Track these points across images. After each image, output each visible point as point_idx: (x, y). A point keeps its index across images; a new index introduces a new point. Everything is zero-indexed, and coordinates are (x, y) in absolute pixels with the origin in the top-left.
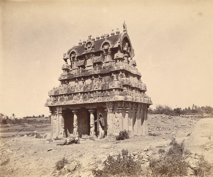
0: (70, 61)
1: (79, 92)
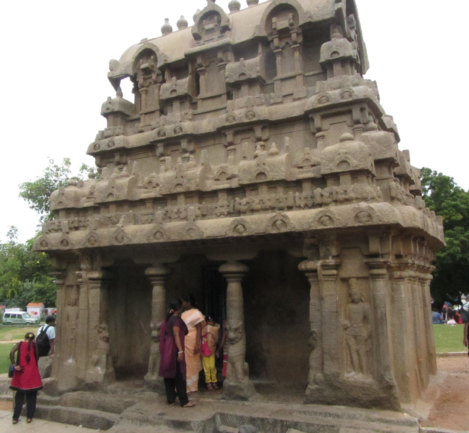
1: (179, 194)
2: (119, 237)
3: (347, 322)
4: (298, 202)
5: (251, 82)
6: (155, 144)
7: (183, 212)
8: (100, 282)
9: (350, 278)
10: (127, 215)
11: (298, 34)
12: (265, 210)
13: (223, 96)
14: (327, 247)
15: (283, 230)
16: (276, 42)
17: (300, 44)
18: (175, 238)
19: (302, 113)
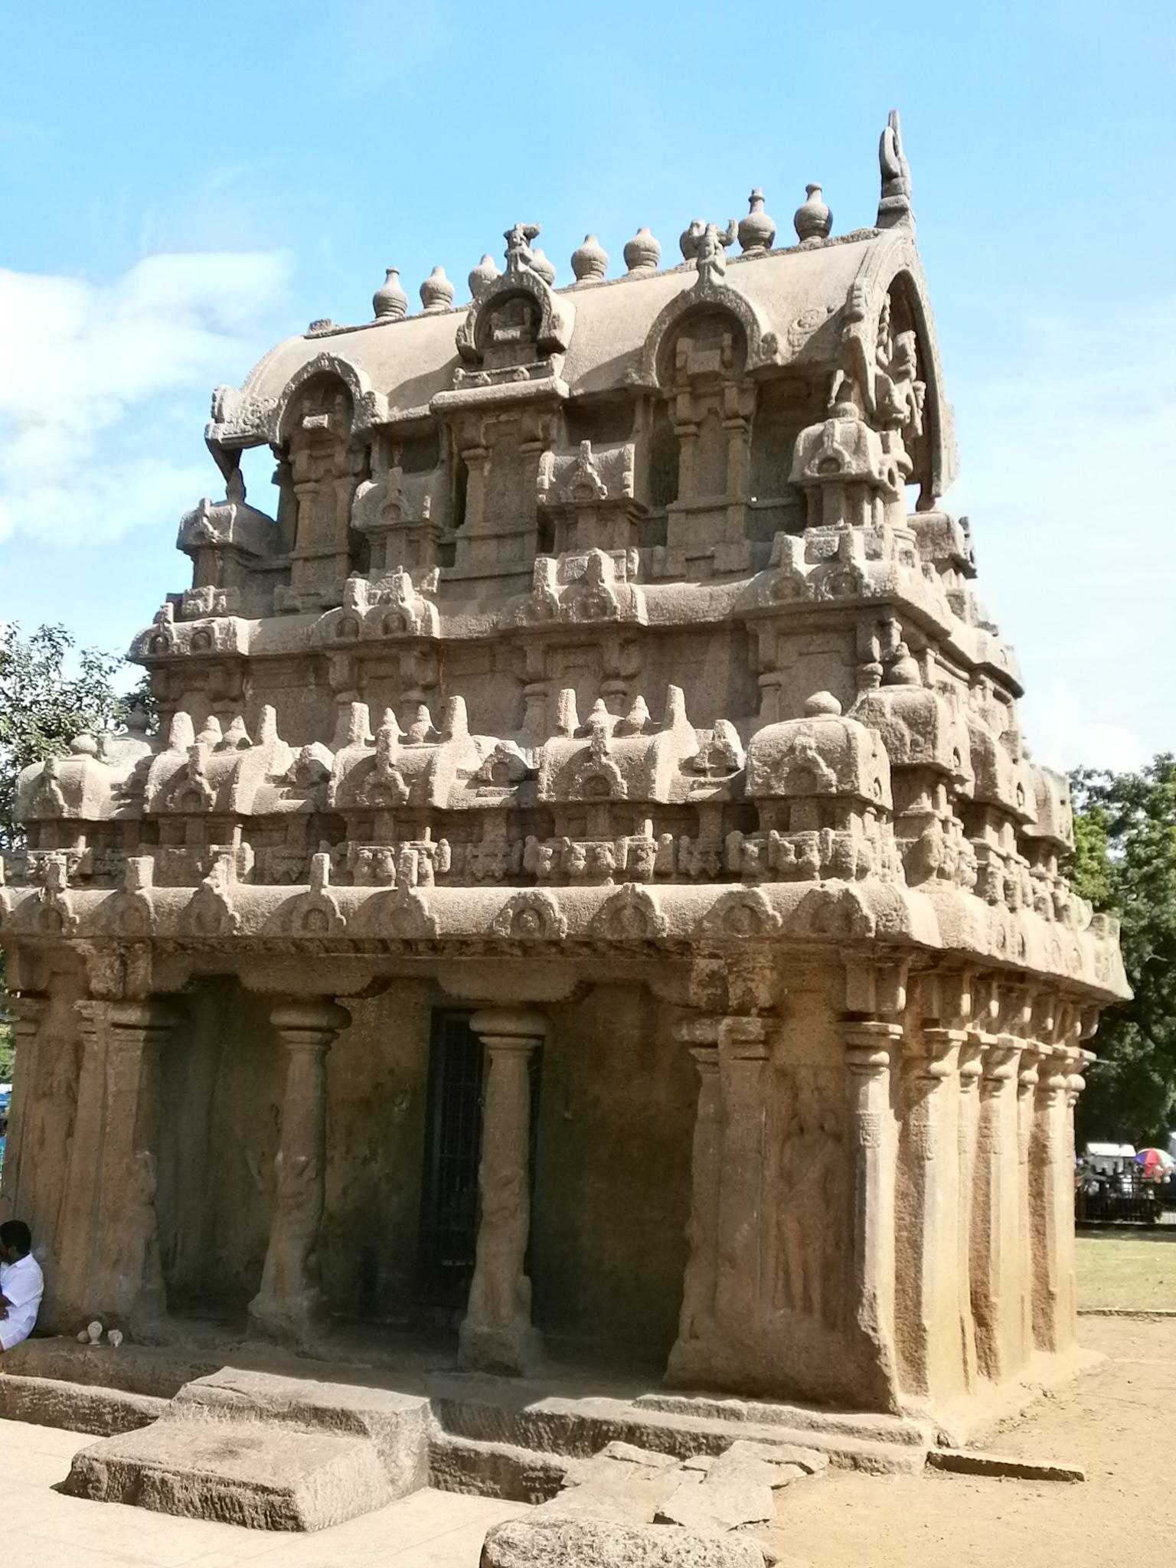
0: (272, 464)
6: (328, 654)
8: (141, 1034)
13: (526, 538)
14: (750, 984)
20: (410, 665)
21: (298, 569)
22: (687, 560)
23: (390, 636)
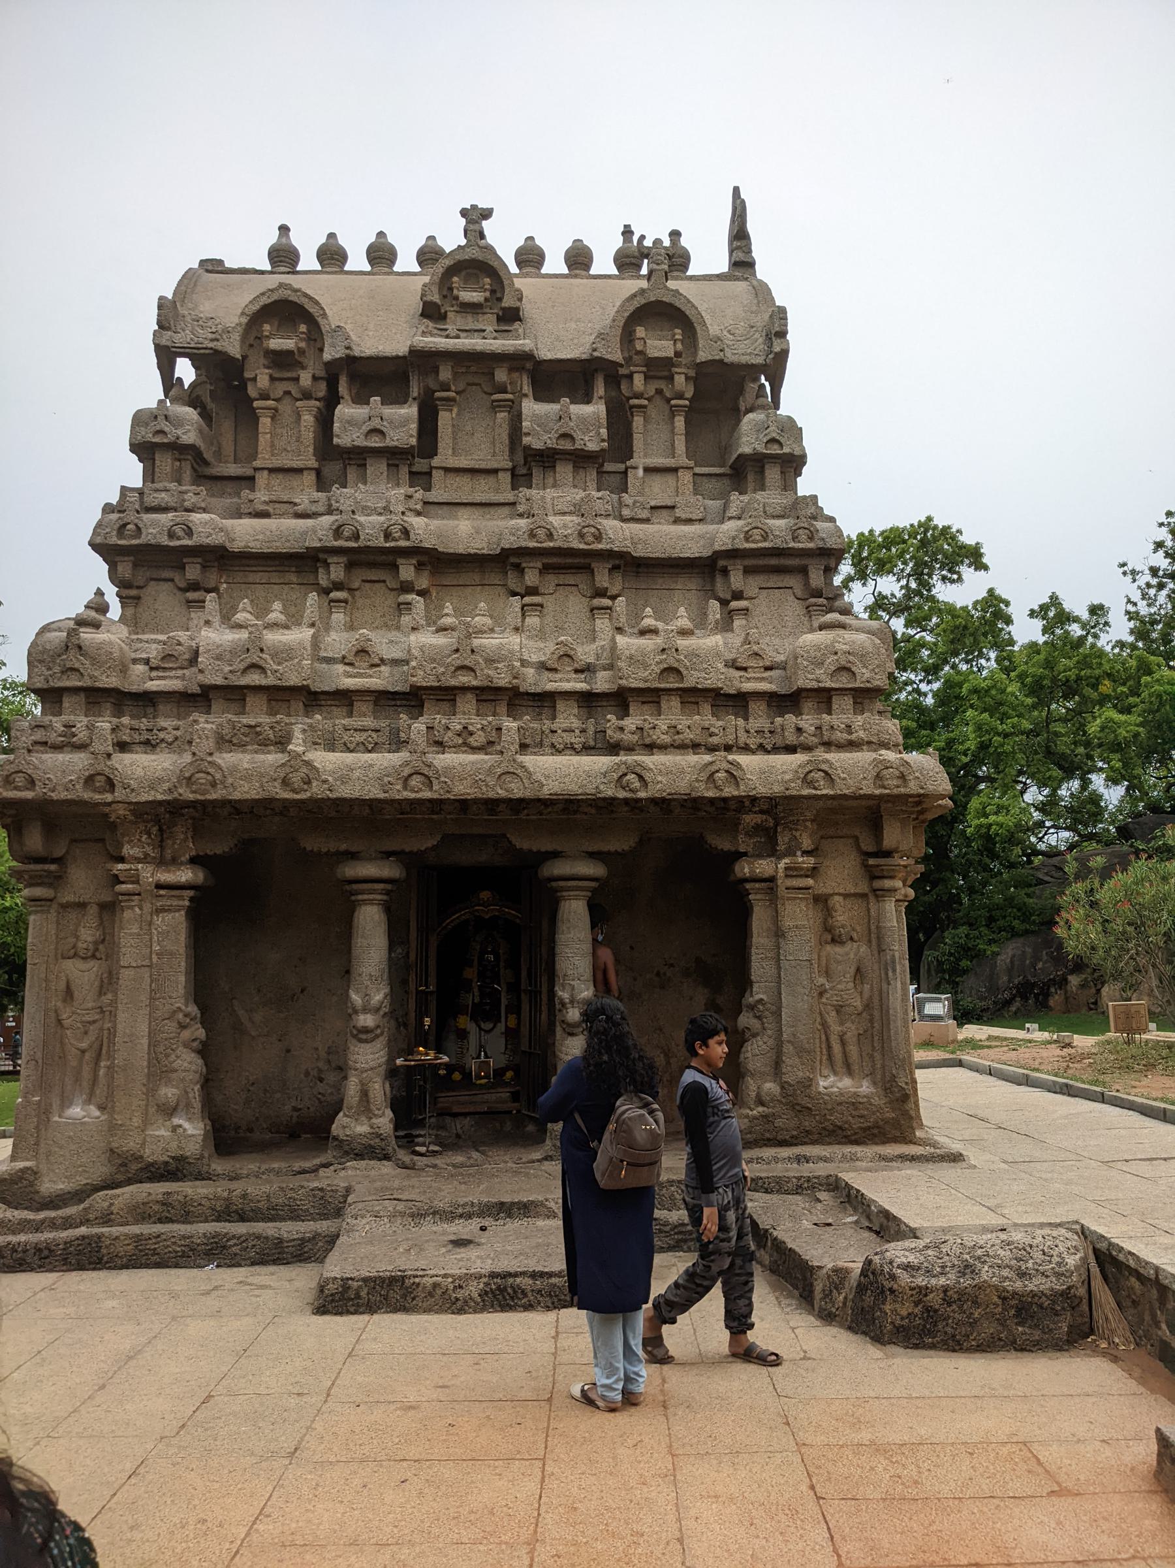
1: (464, 689)
2: (296, 779)
3: (822, 980)
4: (743, 738)
5: (581, 459)
7: (480, 733)
9: (832, 895)
10: (311, 726)
11: (687, 378)
12: (682, 747)
15: (729, 791)
16: (638, 381)
17: (690, 400)
18: (462, 789)
19: (707, 553)
20: (407, 571)
21: (262, 479)
22: (652, 508)
23: (392, 544)
